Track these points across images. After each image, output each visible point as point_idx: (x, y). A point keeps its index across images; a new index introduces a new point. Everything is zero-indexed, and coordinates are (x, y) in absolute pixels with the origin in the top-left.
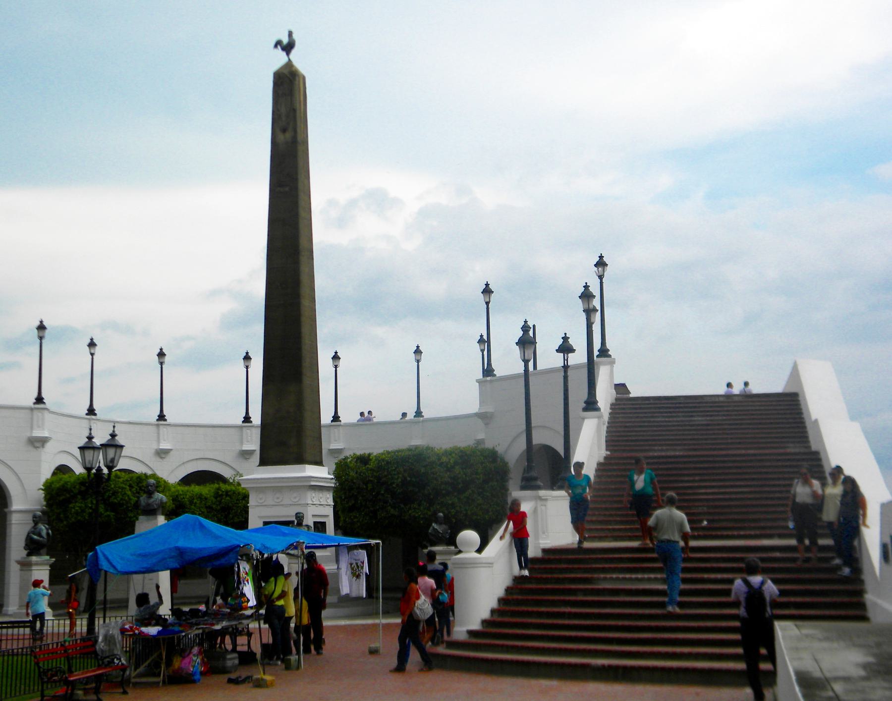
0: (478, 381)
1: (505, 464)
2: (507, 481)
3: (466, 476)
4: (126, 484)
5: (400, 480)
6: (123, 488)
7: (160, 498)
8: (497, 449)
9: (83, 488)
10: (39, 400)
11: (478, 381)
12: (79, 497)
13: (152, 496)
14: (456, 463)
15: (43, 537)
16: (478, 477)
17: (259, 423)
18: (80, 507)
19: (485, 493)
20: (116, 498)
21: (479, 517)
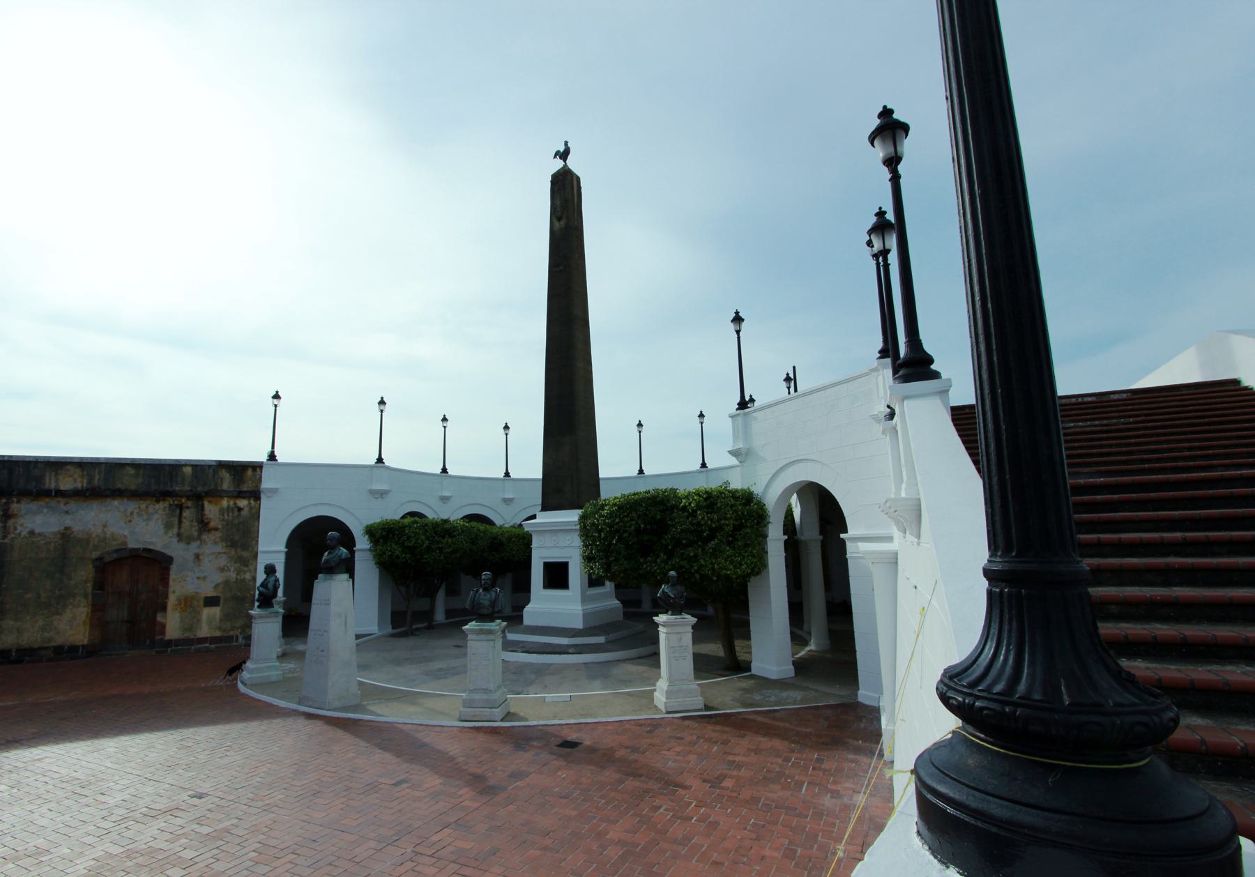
0: (732, 417)
1: (761, 506)
2: (766, 525)
3: (712, 522)
4: (420, 529)
5: (633, 528)
6: (416, 533)
7: (339, 554)
8: (752, 489)
9: (384, 533)
10: (380, 460)
11: (732, 417)
12: (381, 541)
13: (332, 551)
14: (699, 507)
15: (269, 590)
16: (727, 522)
17: (536, 472)
18: (381, 550)
19: (736, 543)
20: (410, 542)
21: (729, 572)
